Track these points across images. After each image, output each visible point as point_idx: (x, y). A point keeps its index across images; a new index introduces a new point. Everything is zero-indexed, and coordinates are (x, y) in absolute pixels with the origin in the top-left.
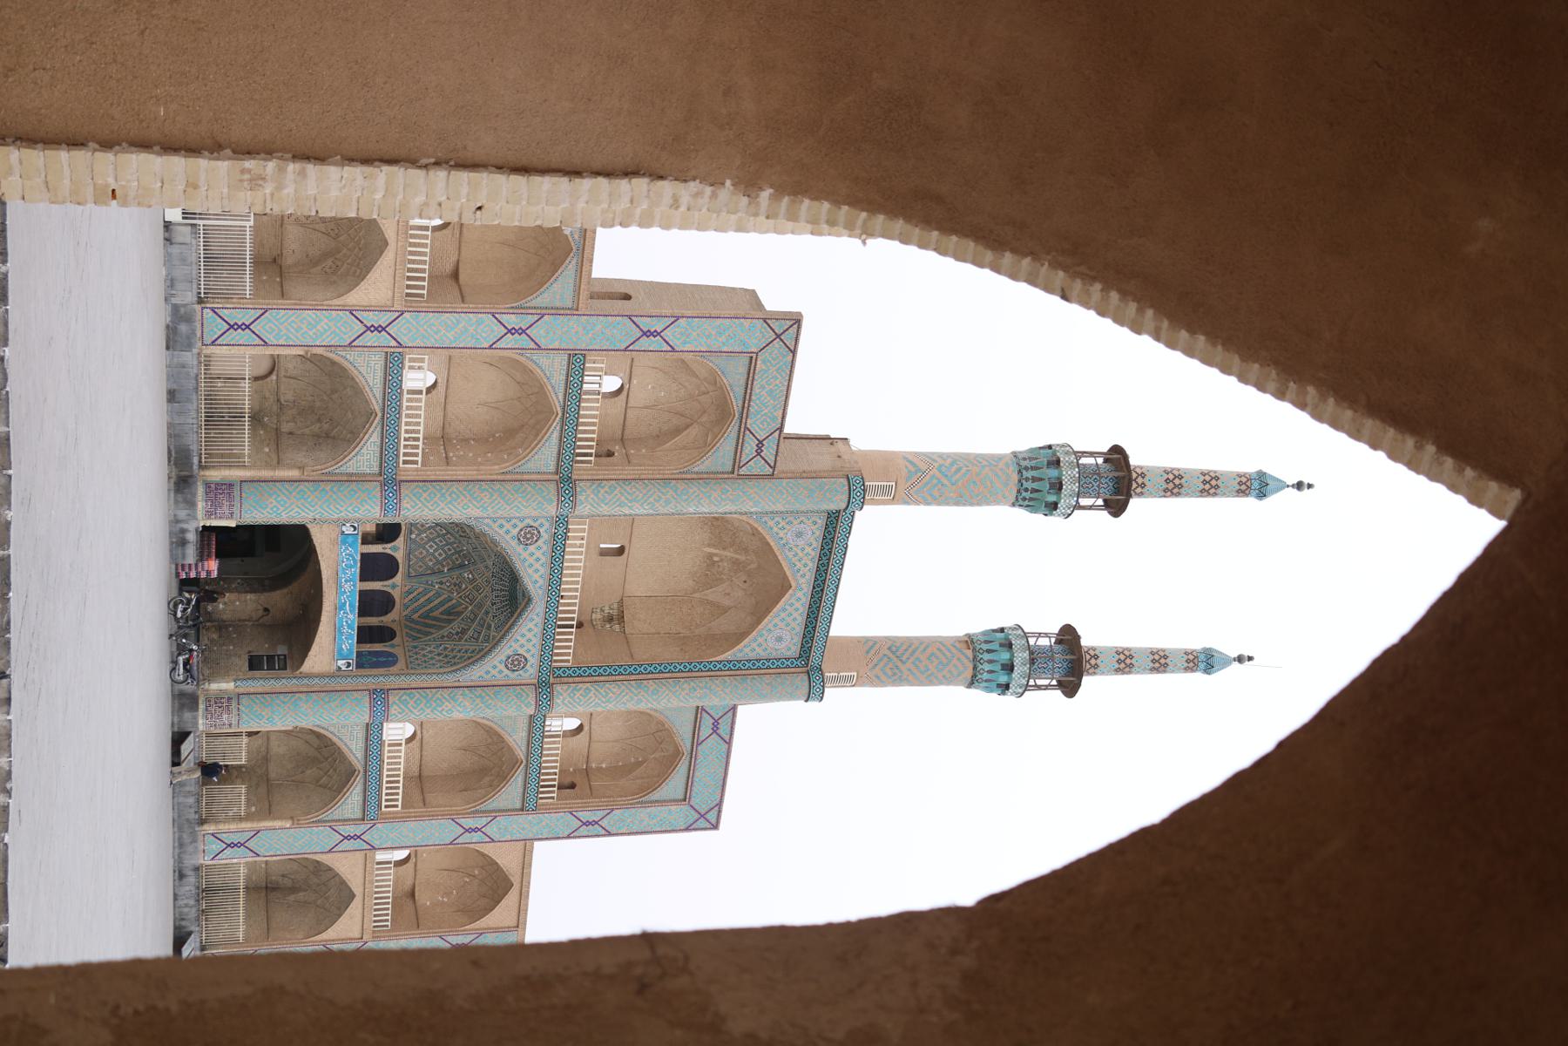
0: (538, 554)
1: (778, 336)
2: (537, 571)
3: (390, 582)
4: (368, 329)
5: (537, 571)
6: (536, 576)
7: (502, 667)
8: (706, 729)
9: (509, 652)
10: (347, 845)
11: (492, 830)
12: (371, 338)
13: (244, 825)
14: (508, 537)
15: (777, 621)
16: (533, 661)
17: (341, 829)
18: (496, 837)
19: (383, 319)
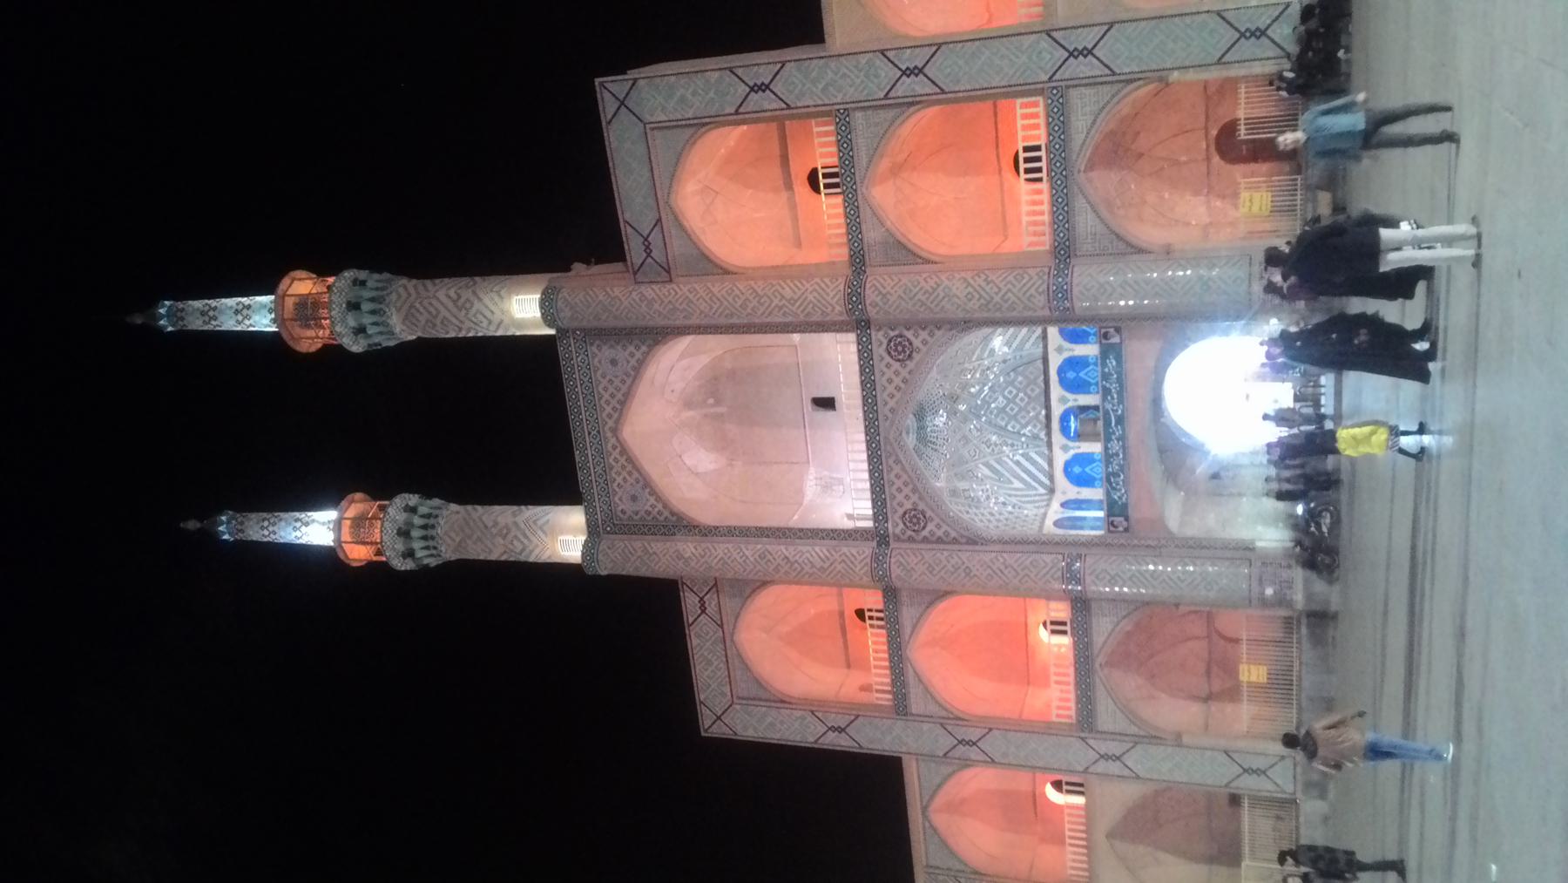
0: (900, 497)
1: (719, 718)
2: (898, 476)
3: (1066, 355)
4: (1118, 758)
5: (898, 476)
6: (897, 469)
7: (917, 343)
8: (655, 239)
9: (911, 365)
10: (1086, 39)
11: (887, 73)
12: (1114, 748)
13: (1235, 71)
14: (937, 520)
15: (624, 389)
16: (879, 351)
17: (1099, 70)
18: (879, 61)
19: (1102, 767)
